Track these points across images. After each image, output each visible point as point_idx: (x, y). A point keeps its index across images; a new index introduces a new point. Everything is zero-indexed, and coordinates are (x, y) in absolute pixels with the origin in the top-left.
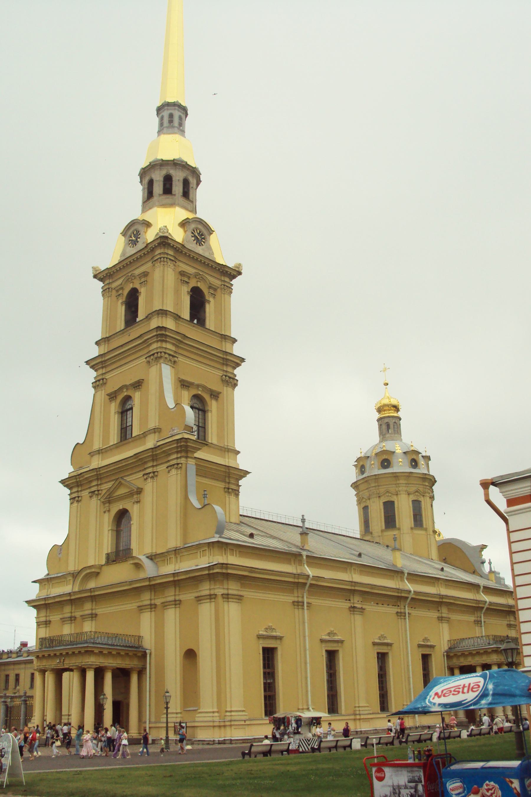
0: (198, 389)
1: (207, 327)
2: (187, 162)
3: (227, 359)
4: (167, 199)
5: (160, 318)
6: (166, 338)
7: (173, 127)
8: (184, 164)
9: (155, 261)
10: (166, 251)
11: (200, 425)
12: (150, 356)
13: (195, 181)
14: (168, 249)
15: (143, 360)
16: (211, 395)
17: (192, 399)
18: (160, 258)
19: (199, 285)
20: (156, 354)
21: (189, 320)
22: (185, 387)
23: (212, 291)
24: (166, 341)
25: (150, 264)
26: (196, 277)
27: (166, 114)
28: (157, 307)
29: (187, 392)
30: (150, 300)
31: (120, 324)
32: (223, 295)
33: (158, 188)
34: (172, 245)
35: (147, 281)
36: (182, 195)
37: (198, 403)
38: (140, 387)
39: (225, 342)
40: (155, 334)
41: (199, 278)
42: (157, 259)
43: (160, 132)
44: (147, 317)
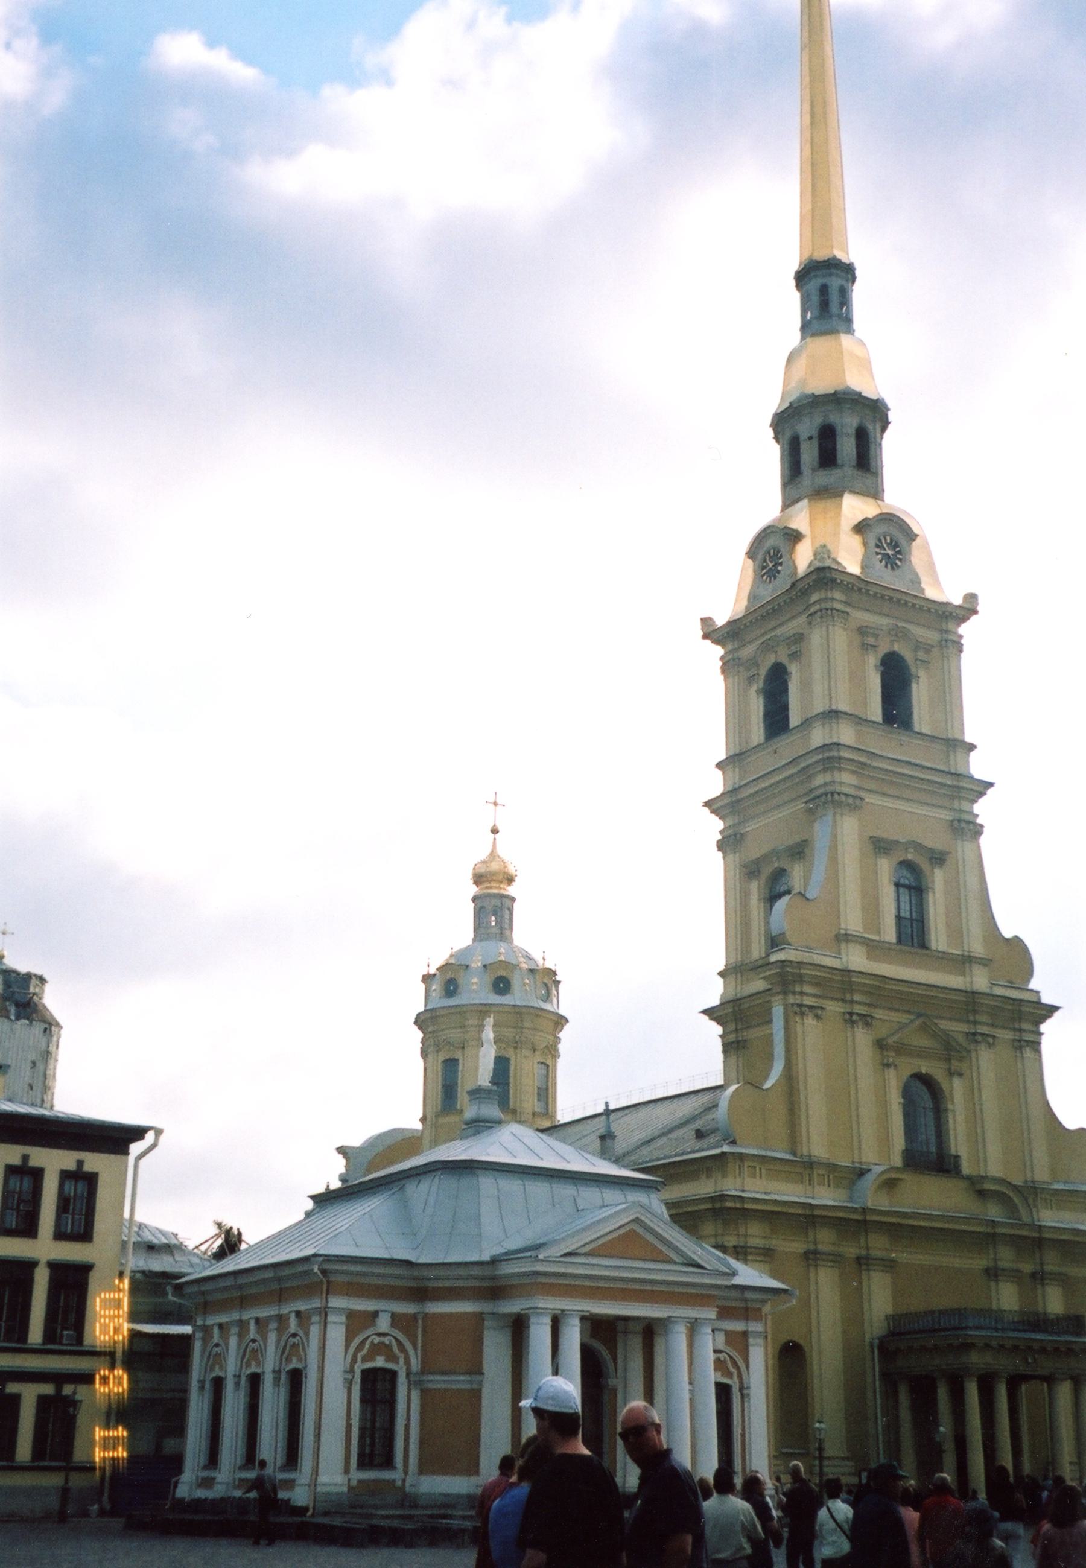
1: (917, 728)
2: (859, 394)
3: (959, 787)
4: (825, 478)
5: (827, 726)
7: (831, 317)
9: (810, 615)
10: (830, 595)
12: (814, 799)
15: (800, 805)
16: (931, 859)
17: (896, 871)
18: (821, 610)
20: (824, 797)
21: (881, 722)
22: (882, 850)
23: (921, 655)
24: (840, 769)
25: (803, 619)
28: (819, 706)
30: (806, 685)
31: (757, 733)
33: (809, 454)
35: (800, 651)
36: (854, 463)
37: (909, 875)
40: (820, 756)
41: (896, 636)
42: (816, 612)
44: (802, 724)
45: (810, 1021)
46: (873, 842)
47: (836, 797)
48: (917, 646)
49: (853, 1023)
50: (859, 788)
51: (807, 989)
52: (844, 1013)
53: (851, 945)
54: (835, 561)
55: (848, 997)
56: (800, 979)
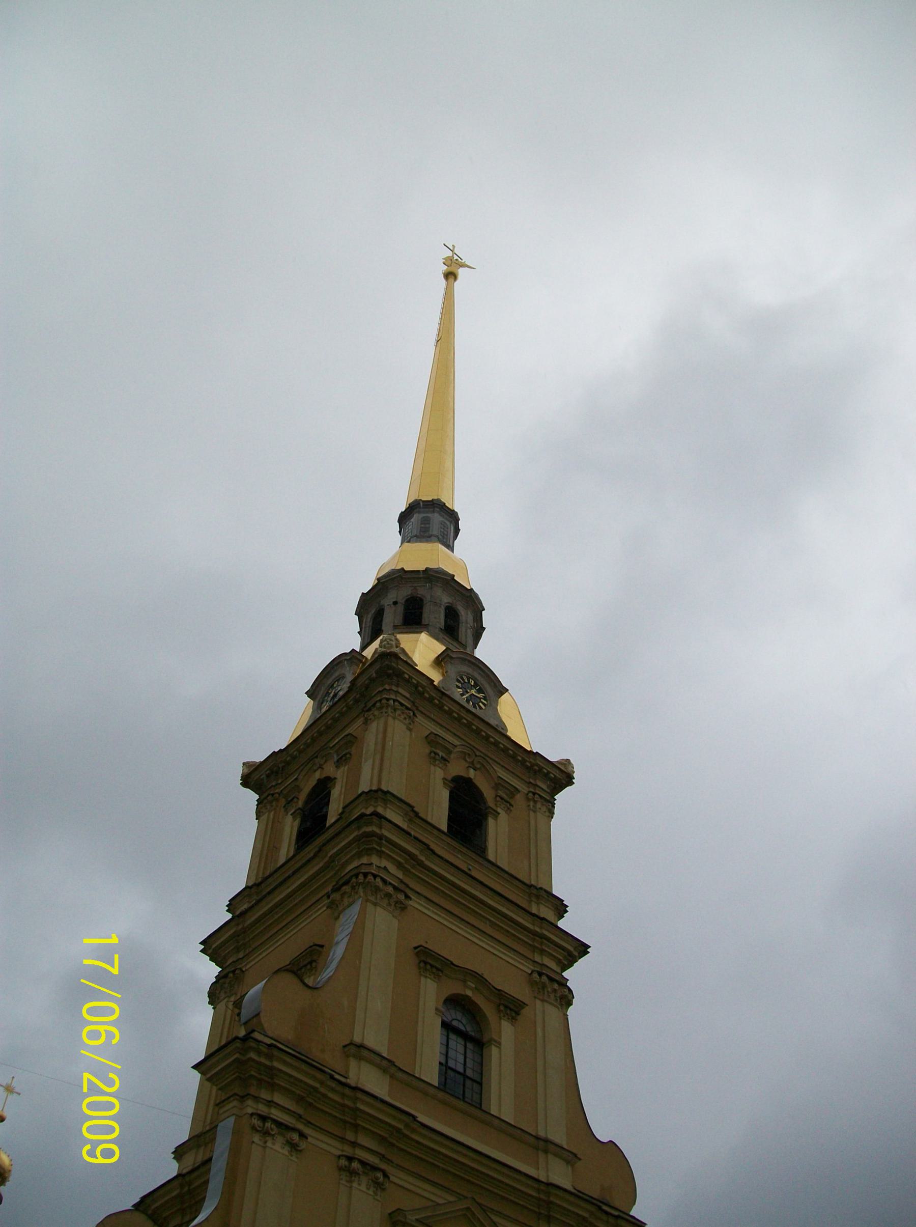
0: (465, 981)
1: (491, 856)
6: (380, 845)
7: (430, 536)
8: (449, 578)
11: (469, 1073)
13: (470, 618)
14: (397, 686)
18: (380, 701)
19: (472, 773)
20: (354, 880)
22: (428, 967)
24: (380, 854)
25: (360, 721)
26: (466, 761)
27: (416, 518)
29: (435, 985)
32: (532, 813)
34: (407, 676)
38: (314, 964)
39: (538, 904)
43: (402, 543)
45: (277, 1146)
46: (417, 954)
47: (370, 877)
48: (499, 784)
49: (353, 1173)
50: (402, 881)
51: (278, 1098)
52: (339, 1157)
53: (363, 1064)
54: (403, 650)
55: (350, 1136)
56: (270, 1079)
